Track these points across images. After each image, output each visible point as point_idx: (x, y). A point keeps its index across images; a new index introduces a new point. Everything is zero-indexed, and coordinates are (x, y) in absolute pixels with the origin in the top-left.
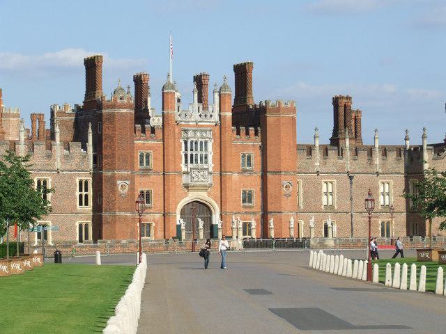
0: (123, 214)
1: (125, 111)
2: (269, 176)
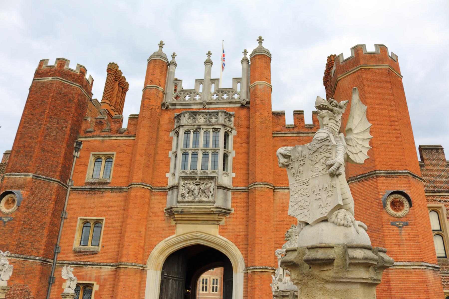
1: (50, 78)
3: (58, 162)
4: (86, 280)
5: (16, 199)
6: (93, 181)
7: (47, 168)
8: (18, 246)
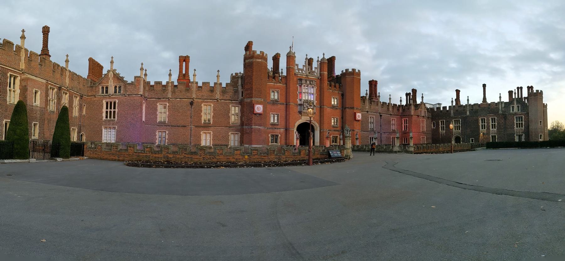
0: (257, 127)
2: (347, 110)
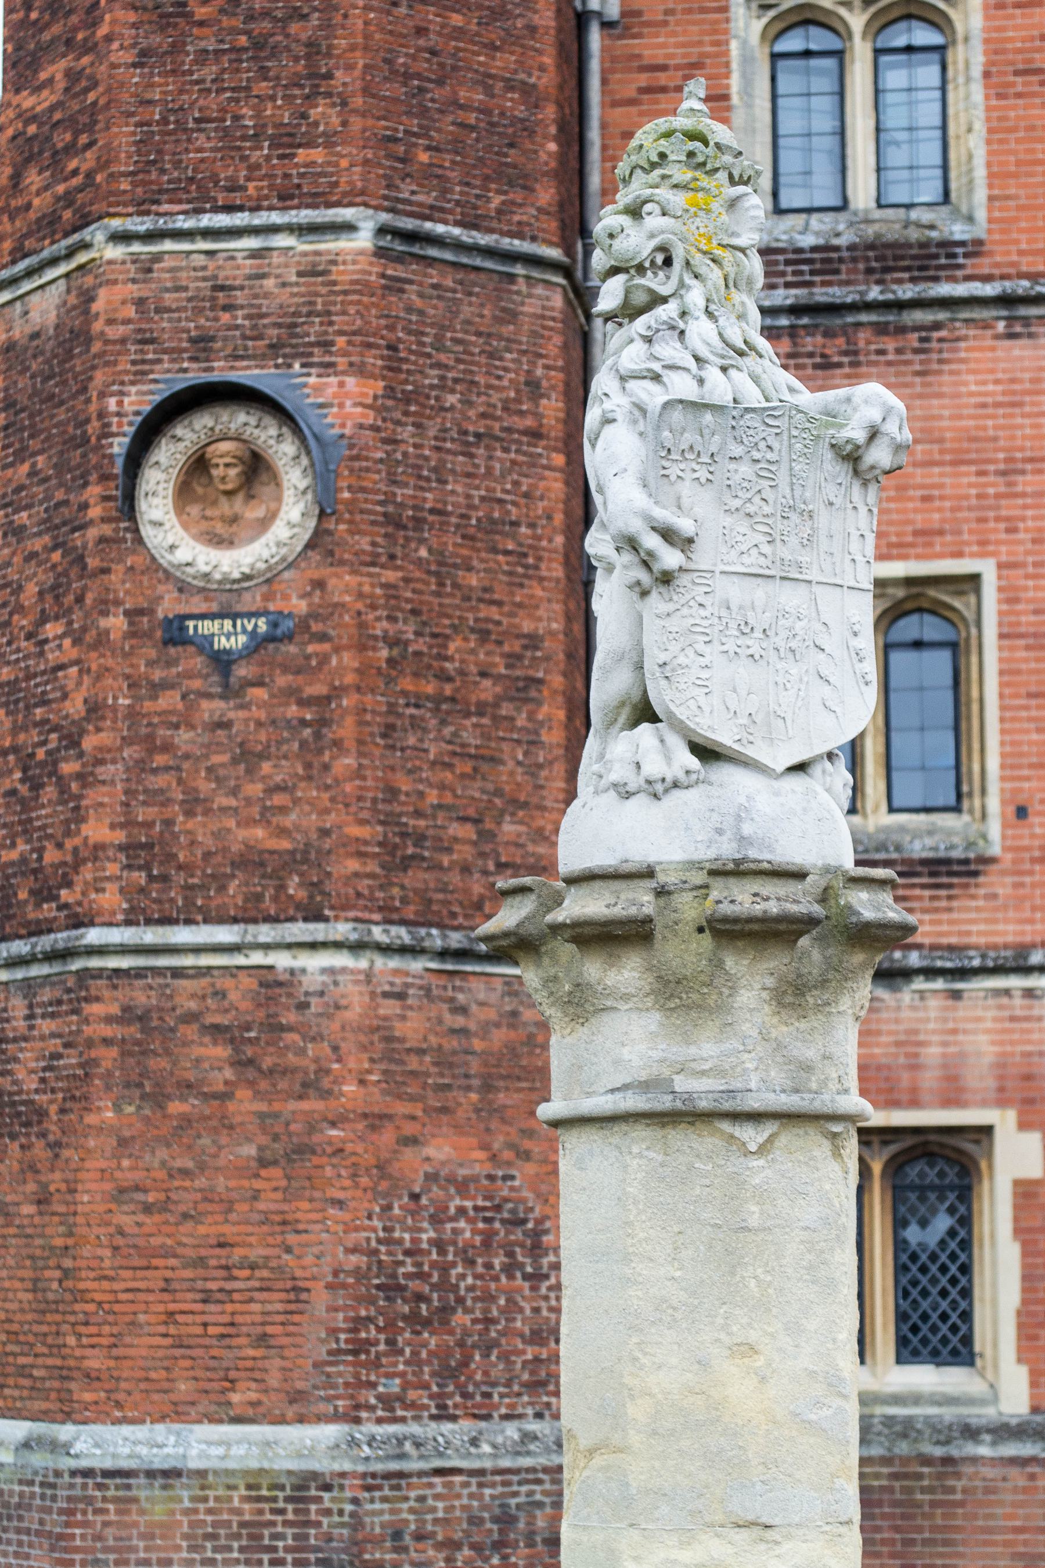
3: (527, 90)
4: (914, 1103)
5: (283, 451)
6: (808, 241)
7: (457, 146)
8: (396, 858)
